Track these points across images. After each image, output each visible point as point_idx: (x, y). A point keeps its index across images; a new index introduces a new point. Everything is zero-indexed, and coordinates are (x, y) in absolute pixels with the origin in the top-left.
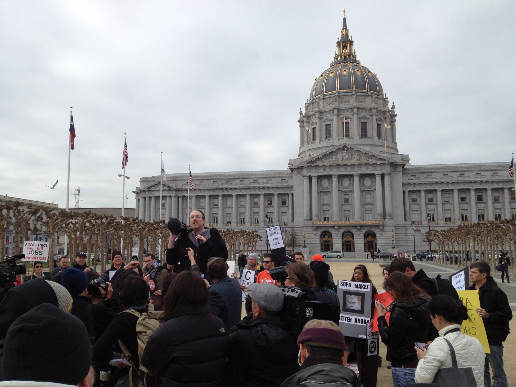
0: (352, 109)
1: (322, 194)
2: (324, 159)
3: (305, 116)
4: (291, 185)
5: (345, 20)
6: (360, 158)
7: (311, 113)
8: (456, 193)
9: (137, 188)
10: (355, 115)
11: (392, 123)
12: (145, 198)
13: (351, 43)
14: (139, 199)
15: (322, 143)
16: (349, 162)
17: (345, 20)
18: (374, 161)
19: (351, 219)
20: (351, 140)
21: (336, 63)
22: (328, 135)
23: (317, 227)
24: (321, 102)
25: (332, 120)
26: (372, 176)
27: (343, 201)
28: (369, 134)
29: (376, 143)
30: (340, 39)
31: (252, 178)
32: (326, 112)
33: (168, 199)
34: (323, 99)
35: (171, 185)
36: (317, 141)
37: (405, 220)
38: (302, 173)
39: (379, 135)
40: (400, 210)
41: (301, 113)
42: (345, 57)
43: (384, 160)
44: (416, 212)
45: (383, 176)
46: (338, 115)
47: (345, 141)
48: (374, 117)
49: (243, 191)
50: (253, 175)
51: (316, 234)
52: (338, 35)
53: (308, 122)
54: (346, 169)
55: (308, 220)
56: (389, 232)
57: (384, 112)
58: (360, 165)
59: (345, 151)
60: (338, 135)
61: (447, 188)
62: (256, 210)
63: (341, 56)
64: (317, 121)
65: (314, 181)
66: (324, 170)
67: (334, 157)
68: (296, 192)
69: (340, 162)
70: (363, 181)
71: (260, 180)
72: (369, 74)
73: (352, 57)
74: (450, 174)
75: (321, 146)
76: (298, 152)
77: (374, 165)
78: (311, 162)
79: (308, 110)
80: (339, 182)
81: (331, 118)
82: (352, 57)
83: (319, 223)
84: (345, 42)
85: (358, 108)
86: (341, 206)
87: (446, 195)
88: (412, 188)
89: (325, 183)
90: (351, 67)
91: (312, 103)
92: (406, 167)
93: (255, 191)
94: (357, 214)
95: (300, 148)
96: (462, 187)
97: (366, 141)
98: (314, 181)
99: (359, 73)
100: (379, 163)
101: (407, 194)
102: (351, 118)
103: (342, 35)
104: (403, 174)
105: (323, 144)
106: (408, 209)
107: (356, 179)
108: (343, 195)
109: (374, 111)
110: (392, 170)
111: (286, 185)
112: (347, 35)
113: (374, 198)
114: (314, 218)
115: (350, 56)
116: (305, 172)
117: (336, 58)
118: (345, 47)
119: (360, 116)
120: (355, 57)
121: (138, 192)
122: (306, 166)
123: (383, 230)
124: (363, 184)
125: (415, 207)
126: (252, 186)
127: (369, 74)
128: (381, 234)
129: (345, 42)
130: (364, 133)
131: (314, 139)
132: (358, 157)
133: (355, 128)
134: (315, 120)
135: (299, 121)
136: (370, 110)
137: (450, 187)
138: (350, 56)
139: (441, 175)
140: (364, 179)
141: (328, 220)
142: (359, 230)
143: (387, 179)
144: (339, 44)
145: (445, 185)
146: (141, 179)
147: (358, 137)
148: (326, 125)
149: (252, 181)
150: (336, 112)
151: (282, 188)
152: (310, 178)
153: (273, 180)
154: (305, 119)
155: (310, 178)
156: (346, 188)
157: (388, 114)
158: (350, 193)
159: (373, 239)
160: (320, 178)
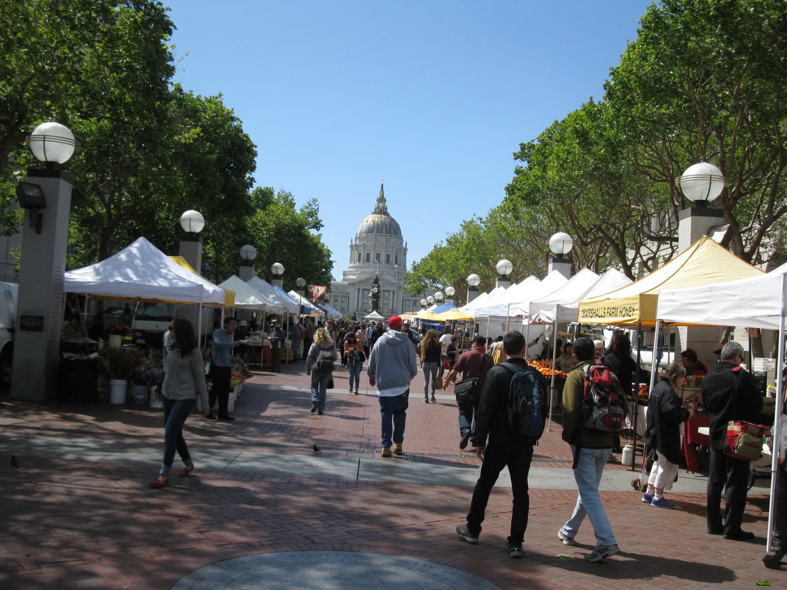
11: (405, 254)
13: (385, 200)
22: (368, 260)
26: (389, 291)
28: (391, 261)
39: (396, 263)
41: (352, 241)
52: (378, 195)
65: (361, 291)
68: (351, 295)
84: (382, 200)
120: (386, 209)
129: (382, 200)
130: (388, 261)
133: (383, 258)
144: (378, 200)
152: (359, 290)
155: (359, 290)
160: (364, 290)
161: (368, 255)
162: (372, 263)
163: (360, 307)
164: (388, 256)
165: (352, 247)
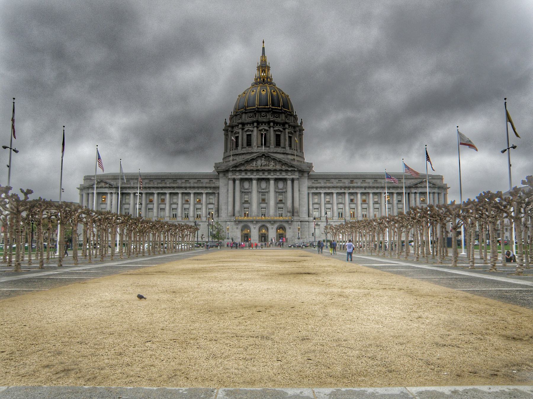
0: (269, 123)
1: (243, 194)
2: (246, 165)
3: (229, 126)
4: (217, 185)
5: (263, 48)
6: (276, 164)
7: (235, 124)
8: (347, 195)
9: (81, 185)
10: (272, 128)
11: (301, 135)
12: (88, 194)
13: (269, 68)
14: (82, 195)
15: (243, 149)
16: (266, 168)
17: (263, 48)
18: (287, 168)
19: (266, 215)
20: (268, 149)
21: (256, 84)
22: (249, 144)
23: (239, 221)
24: (244, 115)
25: (252, 131)
26: (284, 180)
27: (261, 200)
28: (282, 145)
29: (287, 152)
30: (259, 64)
31: (184, 179)
32: (248, 123)
33: (109, 195)
34: (246, 113)
35: (112, 183)
36: (240, 147)
37: (309, 216)
38: (227, 175)
39: (290, 146)
40: (305, 209)
41: (226, 123)
42: (264, 80)
43: (294, 167)
44: (317, 210)
45: (293, 180)
46: (257, 128)
47: (263, 149)
48: (287, 131)
49: (176, 190)
50: (184, 176)
51: (237, 228)
53: (232, 132)
54: (263, 173)
55: (231, 216)
56: (296, 225)
57: (294, 127)
58: (275, 171)
59: (263, 159)
60: (257, 144)
61: (341, 191)
62: (186, 206)
63: (260, 78)
64: (240, 131)
65: (237, 182)
66: (246, 173)
67: (254, 163)
69: (259, 168)
70: (277, 184)
71: (191, 181)
72: (283, 95)
73: (269, 80)
74: (343, 180)
75: (242, 152)
76: (223, 157)
77: (287, 171)
78: (236, 166)
79: (232, 121)
80: (257, 184)
81: (251, 129)
82: (269, 80)
83: (240, 218)
85: (274, 122)
86: (259, 204)
87: (340, 197)
88: (314, 191)
89: (246, 185)
90: (268, 88)
91: (236, 115)
92: (311, 173)
93: (186, 190)
94: (272, 211)
95: (224, 153)
96: (351, 191)
97: (279, 150)
98: (237, 182)
99: (275, 94)
100: (290, 169)
101: (311, 195)
102: (267, 130)
103: (262, 61)
104: (308, 179)
105: (244, 151)
106: (311, 207)
107: (272, 182)
108: (260, 195)
109: (287, 126)
110: (300, 175)
111: (213, 185)
112: (265, 61)
113: (286, 198)
114: (237, 214)
115: (267, 78)
116: (230, 175)
117: (256, 79)
118: (263, 71)
119: (276, 129)
120: (271, 79)
121: (82, 189)
122: (231, 170)
123: (290, 224)
124: (277, 186)
125: (316, 206)
126: (183, 185)
127: (283, 95)
128: (290, 228)
129: (264, 67)
130: (278, 144)
131: (237, 146)
132: (274, 164)
134: (238, 130)
135: (224, 130)
136: (284, 124)
137: (343, 191)
138: (267, 78)
139: (337, 180)
140: (278, 182)
141: (248, 216)
142: (272, 224)
143: (296, 182)
144: (258, 68)
145: (339, 189)
146: (85, 177)
147: (273, 147)
148: (247, 135)
149: (184, 181)
150: (255, 124)
151: (210, 188)
152: (234, 180)
153: (202, 180)
154: (230, 129)
155: (234, 180)
156: (263, 189)
157: (298, 129)
158: (266, 194)
159: (283, 232)
160: (242, 180)
161: (249, 136)
162: (255, 149)
163: (237, 208)
164: (278, 137)
165: (226, 130)
